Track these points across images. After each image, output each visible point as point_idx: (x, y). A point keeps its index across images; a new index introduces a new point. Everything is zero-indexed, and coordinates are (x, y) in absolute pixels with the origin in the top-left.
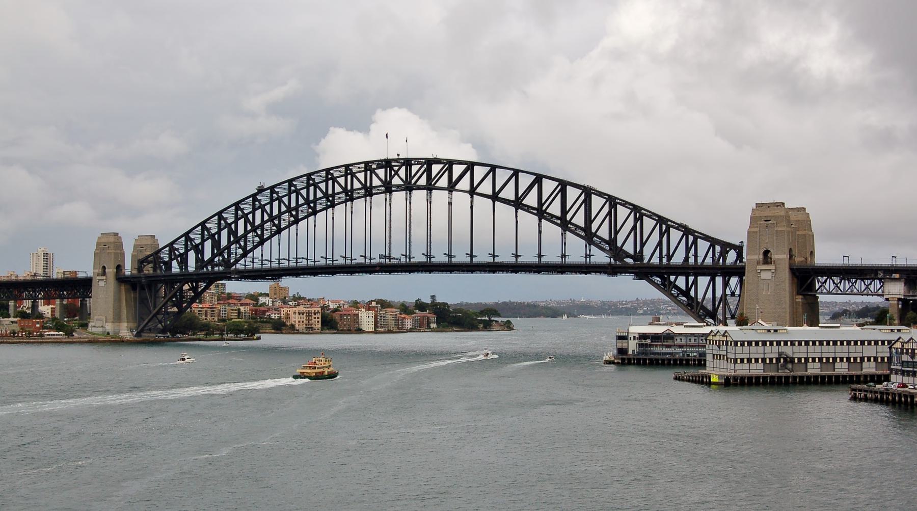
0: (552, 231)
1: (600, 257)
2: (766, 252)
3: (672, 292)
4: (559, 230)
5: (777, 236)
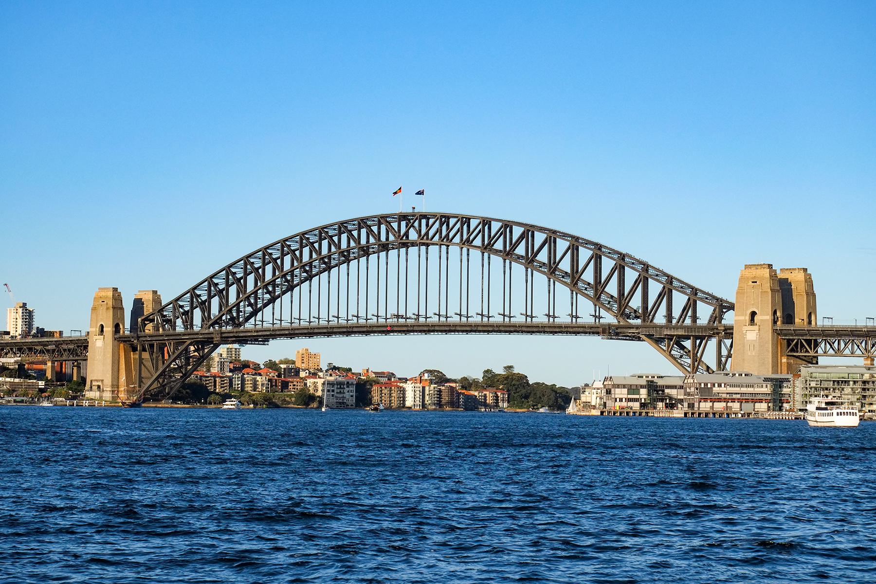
0: (563, 291)
1: (608, 318)
2: (753, 314)
3: (673, 352)
4: (567, 290)
5: (761, 298)
